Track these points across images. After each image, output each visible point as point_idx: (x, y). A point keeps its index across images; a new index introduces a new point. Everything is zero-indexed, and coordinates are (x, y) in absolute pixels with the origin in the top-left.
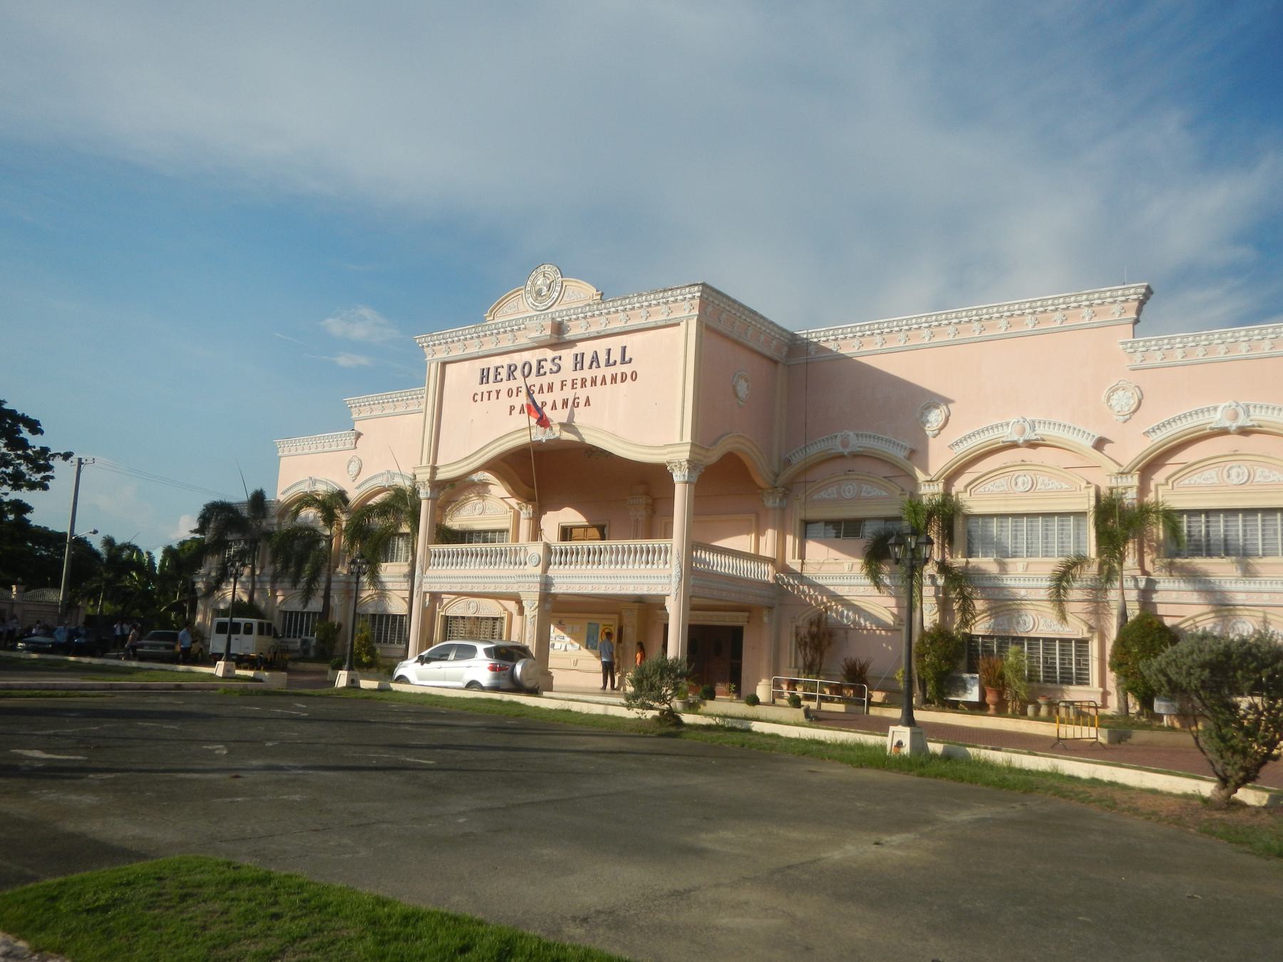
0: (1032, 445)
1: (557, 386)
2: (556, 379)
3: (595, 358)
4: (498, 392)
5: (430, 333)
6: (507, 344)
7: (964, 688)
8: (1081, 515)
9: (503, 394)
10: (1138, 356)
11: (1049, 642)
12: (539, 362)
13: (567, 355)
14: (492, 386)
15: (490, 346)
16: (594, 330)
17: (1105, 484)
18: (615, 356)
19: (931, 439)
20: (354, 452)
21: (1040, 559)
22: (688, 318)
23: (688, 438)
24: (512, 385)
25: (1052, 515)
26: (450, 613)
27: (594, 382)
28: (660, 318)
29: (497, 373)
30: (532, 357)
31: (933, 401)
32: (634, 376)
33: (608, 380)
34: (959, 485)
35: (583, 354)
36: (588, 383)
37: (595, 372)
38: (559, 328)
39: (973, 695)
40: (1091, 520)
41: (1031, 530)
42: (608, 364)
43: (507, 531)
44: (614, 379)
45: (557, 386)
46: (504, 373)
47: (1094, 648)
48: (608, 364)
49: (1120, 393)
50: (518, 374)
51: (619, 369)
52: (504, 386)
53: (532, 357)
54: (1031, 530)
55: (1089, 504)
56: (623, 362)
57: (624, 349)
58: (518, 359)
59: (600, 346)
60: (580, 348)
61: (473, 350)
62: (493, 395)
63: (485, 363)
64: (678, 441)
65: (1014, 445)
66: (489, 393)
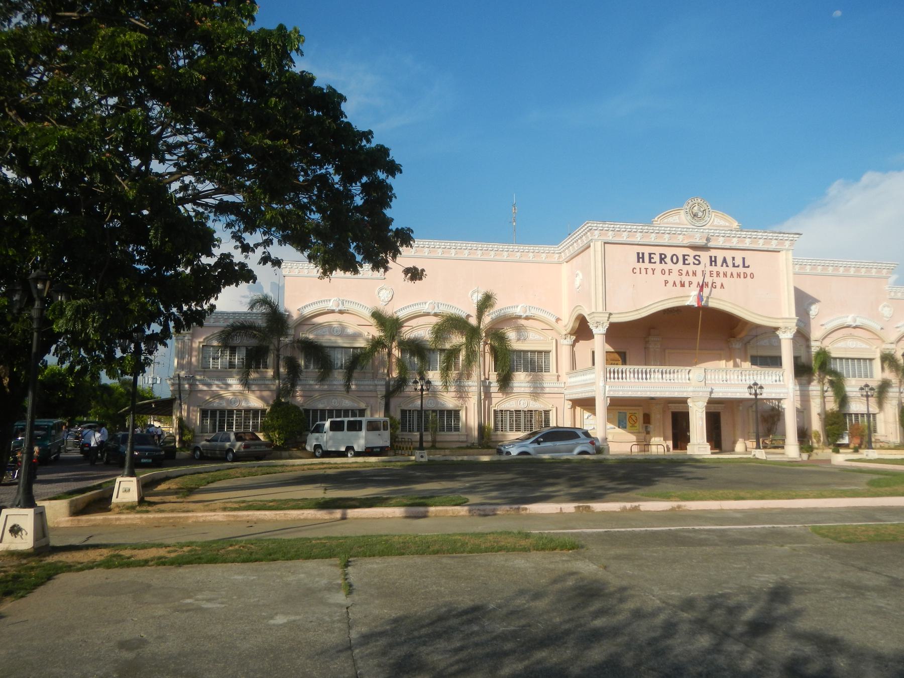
1: (699, 273)
2: (699, 269)
3: (725, 260)
4: (653, 270)
5: (604, 222)
6: (666, 240)
7: (842, 438)
8: (871, 360)
9: (658, 272)
10: (892, 294)
11: (862, 415)
12: (684, 256)
13: (705, 256)
14: (646, 264)
15: (652, 239)
16: (728, 245)
17: (884, 346)
18: (739, 261)
20: (382, 284)
21: (857, 378)
22: (788, 250)
23: (794, 315)
24: (666, 267)
25: (859, 359)
26: (498, 408)
27: (725, 275)
28: (773, 245)
29: (650, 258)
30: (680, 252)
31: (815, 301)
32: (752, 276)
33: (735, 275)
35: (715, 257)
36: (721, 275)
37: (724, 268)
38: (708, 240)
39: (846, 440)
40: (877, 364)
41: (853, 365)
42: (734, 266)
43: (547, 352)
44: (739, 275)
45: (699, 273)
46: (656, 258)
47: (880, 418)
48: (734, 266)
49: (886, 309)
50: (668, 260)
51: (741, 270)
52: (659, 267)
53: (680, 252)
54: (853, 365)
55: (878, 356)
56: (744, 266)
57: (744, 259)
58: (669, 252)
59: (729, 255)
60: (713, 253)
61: (638, 238)
62: (650, 271)
63: (641, 249)
64: (787, 316)
66: (646, 269)
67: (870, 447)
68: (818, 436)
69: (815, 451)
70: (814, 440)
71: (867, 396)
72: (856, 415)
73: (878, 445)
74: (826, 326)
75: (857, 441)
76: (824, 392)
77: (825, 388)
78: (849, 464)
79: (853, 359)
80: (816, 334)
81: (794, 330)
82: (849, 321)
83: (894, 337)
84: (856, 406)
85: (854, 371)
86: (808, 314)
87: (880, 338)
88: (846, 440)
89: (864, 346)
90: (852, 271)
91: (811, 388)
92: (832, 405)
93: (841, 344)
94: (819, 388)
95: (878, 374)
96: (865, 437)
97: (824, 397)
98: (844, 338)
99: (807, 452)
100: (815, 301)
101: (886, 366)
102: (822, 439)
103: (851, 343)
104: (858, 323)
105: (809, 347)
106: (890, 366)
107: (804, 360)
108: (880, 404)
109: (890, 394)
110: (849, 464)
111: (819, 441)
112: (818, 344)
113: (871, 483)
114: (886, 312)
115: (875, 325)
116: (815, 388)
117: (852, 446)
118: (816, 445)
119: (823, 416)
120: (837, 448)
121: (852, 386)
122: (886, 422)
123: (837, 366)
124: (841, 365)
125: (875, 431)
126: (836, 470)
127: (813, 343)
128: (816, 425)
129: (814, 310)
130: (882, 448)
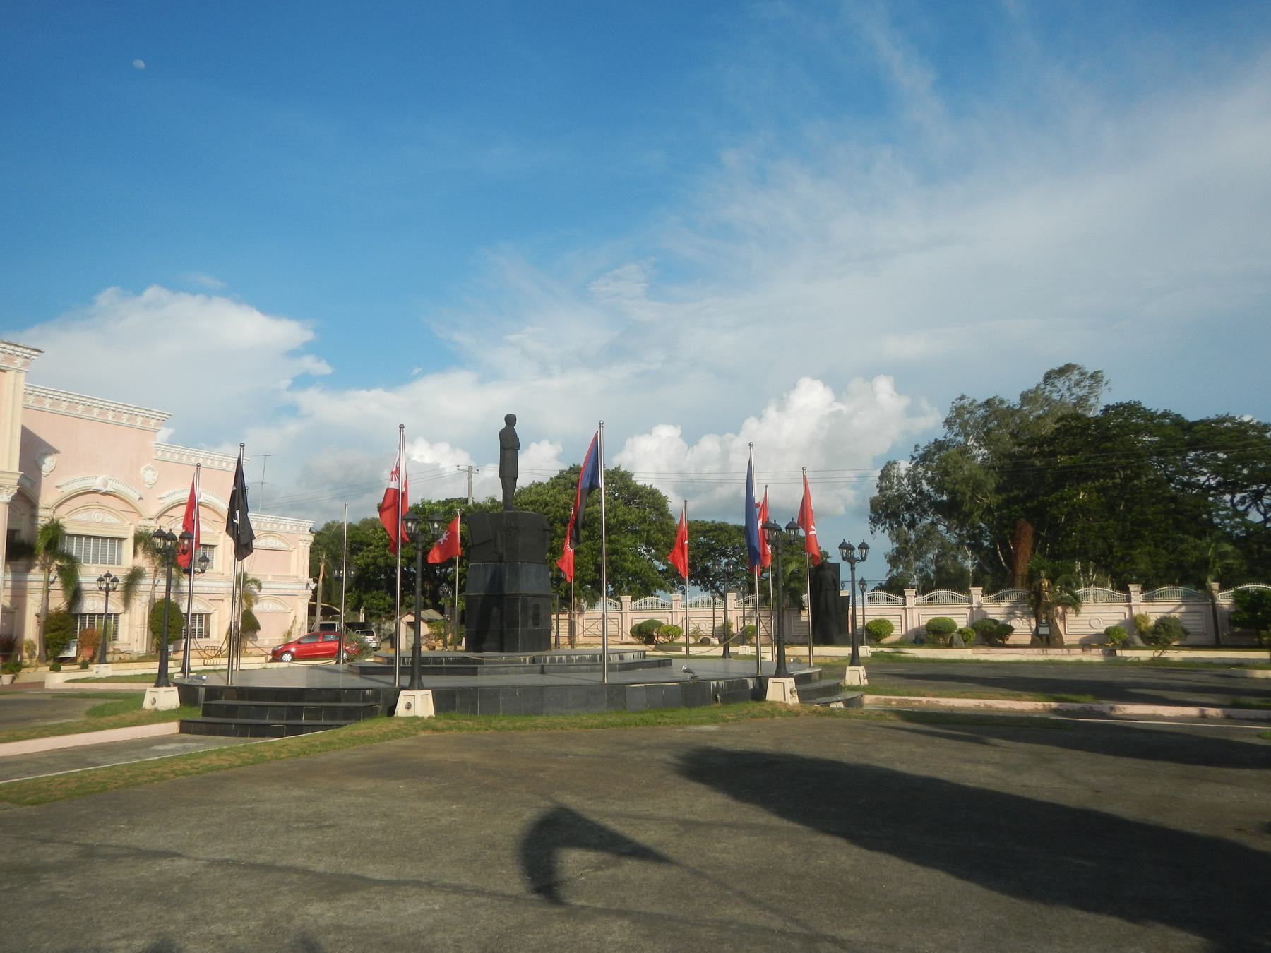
0: (105, 494)
7: (68, 649)
8: (121, 539)
10: (160, 453)
11: (100, 615)
17: (142, 522)
19: (43, 479)
22: (18, 371)
23: (15, 468)
25: (105, 538)
31: (51, 451)
34: (61, 512)
39: (72, 653)
40: (129, 545)
41: (96, 546)
47: (124, 619)
49: (149, 472)
54: (96, 546)
55: (130, 536)
64: (5, 469)
65: (95, 492)
67: (103, 661)
68: (31, 646)
69: (24, 670)
70: (25, 654)
71: (107, 590)
72: (92, 616)
73: (116, 657)
74: (64, 489)
75: (87, 653)
76: (48, 583)
77: (52, 578)
78: (70, 686)
79: (96, 538)
80: (47, 498)
81: (13, 491)
82: (98, 484)
83: (154, 511)
84: (92, 604)
85: (95, 555)
86: (40, 470)
87: (136, 511)
88: (72, 653)
89: (114, 520)
90: (110, 414)
91: (30, 577)
92: (58, 602)
93: (79, 517)
94: (42, 577)
95: (129, 558)
96: (99, 647)
97: (48, 591)
98: (87, 507)
99: (12, 671)
100: (51, 451)
101: (140, 549)
102: (37, 652)
103: (96, 516)
104: (109, 488)
105: (34, 517)
106: (145, 549)
107: (24, 535)
108: (127, 601)
109: (141, 588)
110: (70, 686)
111: (31, 657)
112: (49, 513)
113: (95, 712)
114: (149, 476)
115: (133, 495)
116: (36, 577)
117: (80, 660)
118: (28, 661)
119: (43, 619)
120: (57, 664)
121: (89, 575)
122: (130, 625)
123: (73, 548)
124: (79, 545)
125: (115, 638)
126: (48, 697)
127: (41, 512)
128: (31, 631)
129: (49, 463)
130: (121, 661)
